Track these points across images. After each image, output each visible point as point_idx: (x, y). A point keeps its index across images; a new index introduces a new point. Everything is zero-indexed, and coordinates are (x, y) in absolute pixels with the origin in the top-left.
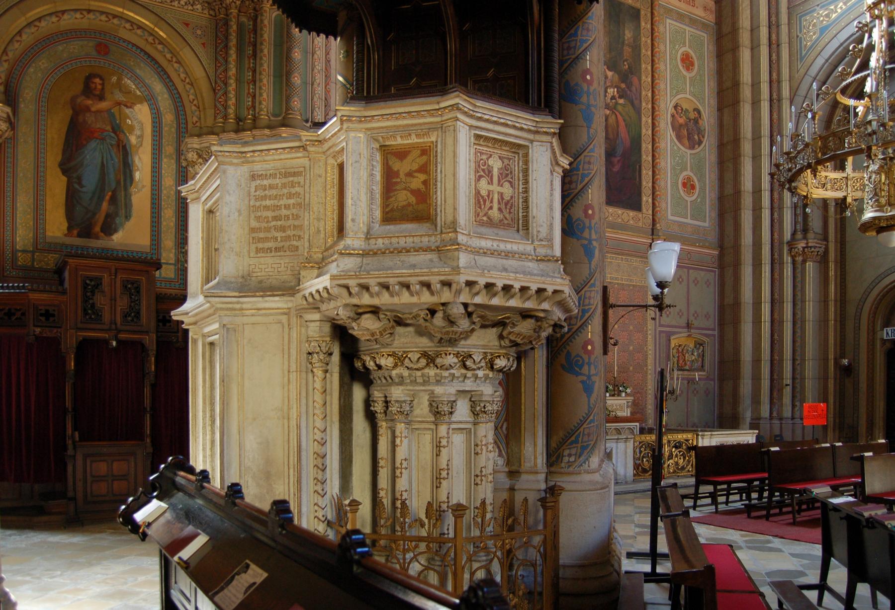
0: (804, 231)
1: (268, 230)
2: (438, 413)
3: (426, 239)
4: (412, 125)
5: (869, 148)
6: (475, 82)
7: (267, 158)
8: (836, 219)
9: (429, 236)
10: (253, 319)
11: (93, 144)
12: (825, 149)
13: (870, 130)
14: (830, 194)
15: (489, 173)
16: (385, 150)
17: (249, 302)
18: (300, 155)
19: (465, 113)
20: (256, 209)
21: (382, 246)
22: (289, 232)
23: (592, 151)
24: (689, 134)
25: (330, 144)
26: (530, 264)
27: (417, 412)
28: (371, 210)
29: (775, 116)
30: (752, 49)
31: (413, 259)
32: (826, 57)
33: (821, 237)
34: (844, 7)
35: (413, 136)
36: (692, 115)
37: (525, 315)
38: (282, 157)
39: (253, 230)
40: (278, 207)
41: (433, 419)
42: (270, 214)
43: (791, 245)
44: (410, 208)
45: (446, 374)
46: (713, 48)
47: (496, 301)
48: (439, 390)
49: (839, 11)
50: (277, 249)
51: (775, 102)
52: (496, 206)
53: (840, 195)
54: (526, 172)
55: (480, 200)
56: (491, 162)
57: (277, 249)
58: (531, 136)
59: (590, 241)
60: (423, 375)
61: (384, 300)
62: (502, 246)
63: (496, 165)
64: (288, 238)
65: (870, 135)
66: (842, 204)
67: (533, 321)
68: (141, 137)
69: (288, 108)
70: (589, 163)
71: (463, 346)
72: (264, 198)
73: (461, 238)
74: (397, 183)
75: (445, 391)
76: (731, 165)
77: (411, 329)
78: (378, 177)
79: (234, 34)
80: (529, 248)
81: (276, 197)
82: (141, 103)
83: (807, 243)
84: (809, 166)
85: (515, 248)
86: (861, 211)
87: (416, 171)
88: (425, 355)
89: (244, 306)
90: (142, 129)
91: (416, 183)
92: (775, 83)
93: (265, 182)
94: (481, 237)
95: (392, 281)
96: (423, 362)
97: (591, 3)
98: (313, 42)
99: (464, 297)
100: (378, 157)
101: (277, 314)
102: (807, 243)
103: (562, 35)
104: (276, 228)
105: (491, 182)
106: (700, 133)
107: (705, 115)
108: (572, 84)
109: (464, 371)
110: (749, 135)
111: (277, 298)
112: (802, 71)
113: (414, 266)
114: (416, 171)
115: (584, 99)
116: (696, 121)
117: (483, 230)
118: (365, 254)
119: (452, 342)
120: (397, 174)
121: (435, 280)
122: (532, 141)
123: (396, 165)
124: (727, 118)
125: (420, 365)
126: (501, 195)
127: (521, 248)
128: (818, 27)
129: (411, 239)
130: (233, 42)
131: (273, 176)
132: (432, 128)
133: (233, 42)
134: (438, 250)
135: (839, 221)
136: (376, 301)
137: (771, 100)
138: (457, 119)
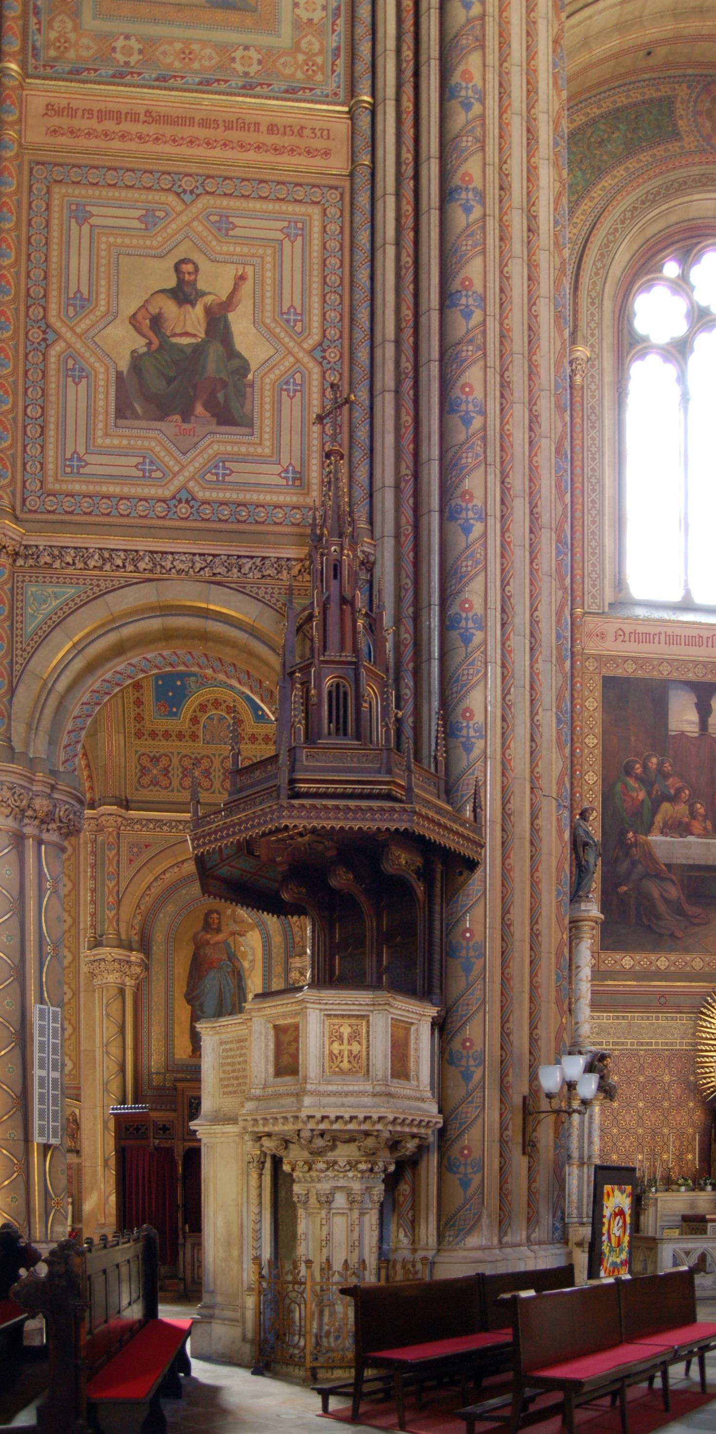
1: (229, 1079)
10: (222, 1140)
11: (212, 974)
15: (340, 1038)
16: (276, 1028)
17: (218, 1128)
20: (222, 1065)
22: (241, 1081)
23: (472, 994)
26: (366, 1099)
28: (266, 1069)
37: (367, 1134)
39: (221, 1080)
40: (234, 1064)
42: (230, 1068)
45: (323, 1175)
47: (336, 1126)
48: (318, 1186)
50: (235, 1092)
52: (346, 1059)
54: (368, 1032)
56: (342, 1029)
57: (235, 1092)
58: (371, 1008)
59: (467, 1068)
62: (346, 1088)
64: (239, 1085)
68: (252, 961)
70: (468, 1005)
71: (331, 1156)
72: (227, 1057)
73: (309, 1087)
78: (272, 1046)
81: (233, 1057)
82: (252, 930)
85: (356, 1088)
90: (254, 954)
91: (292, 1050)
93: (228, 1047)
94: (329, 1083)
95: (268, 1117)
100: (272, 1033)
103: (447, 905)
105: (342, 1043)
113: (283, 1106)
118: (258, 1099)
126: (351, 1052)
127: (362, 1088)
131: (232, 1042)
132: (296, 1014)
136: (266, 1129)
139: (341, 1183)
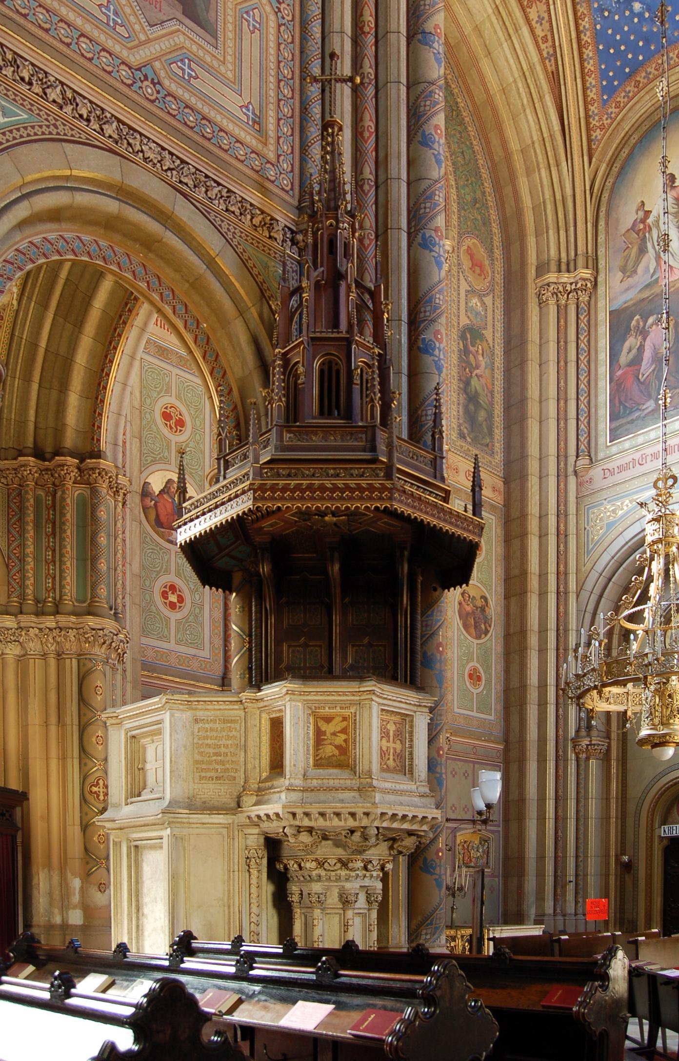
0: (588, 728)
1: (210, 763)
2: (346, 901)
3: (349, 782)
4: (338, 700)
5: (646, 677)
6: (353, 646)
7: (208, 707)
8: (618, 734)
9: (352, 779)
10: (198, 831)
12: (609, 673)
13: (646, 662)
14: (614, 708)
18: (236, 707)
19: (378, 696)
21: (316, 785)
23: (443, 706)
24: (475, 623)
25: (266, 703)
26: (415, 799)
27: (329, 901)
29: (562, 609)
30: (540, 537)
31: (341, 795)
32: (612, 554)
33: (604, 735)
34: (630, 505)
35: (338, 708)
36: (479, 603)
37: (410, 833)
38: (221, 707)
39: (196, 762)
40: (219, 746)
41: (341, 906)
42: (211, 751)
43: (575, 741)
44: (335, 758)
45: (353, 874)
46: (500, 532)
48: (348, 885)
49: (625, 508)
51: (562, 595)
52: (391, 757)
53: (621, 708)
54: (411, 733)
55: (383, 754)
56: (389, 727)
58: (415, 708)
59: (441, 774)
60: (336, 875)
61: (321, 823)
62: (398, 787)
63: (392, 728)
64: (227, 770)
65: (646, 666)
66: (623, 716)
67: (415, 838)
69: (93, 596)
70: (441, 715)
71: (367, 855)
73: (375, 783)
74: (324, 740)
75: (352, 886)
76: (517, 658)
77: (330, 842)
79: (32, 509)
80: (414, 787)
83: (591, 741)
84: (595, 687)
86: (639, 729)
87: (339, 732)
88: (340, 860)
89: (191, 821)
91: (340, 739)
92: (562, 575)
93: (207, 726)
96: (339, 865)
97: (444, 590)
98: (115, 525)
99: (377, 823)
100: (311, 720)
101: (218, 828)
102: (591, 741)
104: (216, 762)
105: (388, 741)
106: (487, 621)
107: (492, 603)
108: (429, 654)
109: (364, 872)
110: (536, 627)
111: (221, 816)
112: (589, 566)
113: (342, 801)
114: (339, 732)
115: (438, 666)
116: (483, 609)
117: (385, 775)
118: (304, 790)
119: (361, 852)
120: (324, 733)
121: (359, 812)
122: (415, 712)
123: (324, 727)
124: (513, 607)
125: (336, 868)
126: (395, 749)
128: (605, 522)
129: (337, 781)
130: (30, 517)
131: (214, 721)
132: (352, 703)
133: (30, 517)
134: (359, 790)
135: (621, 735)
137: (558, 593)
138: (372, 700)
139: (367, 882)
